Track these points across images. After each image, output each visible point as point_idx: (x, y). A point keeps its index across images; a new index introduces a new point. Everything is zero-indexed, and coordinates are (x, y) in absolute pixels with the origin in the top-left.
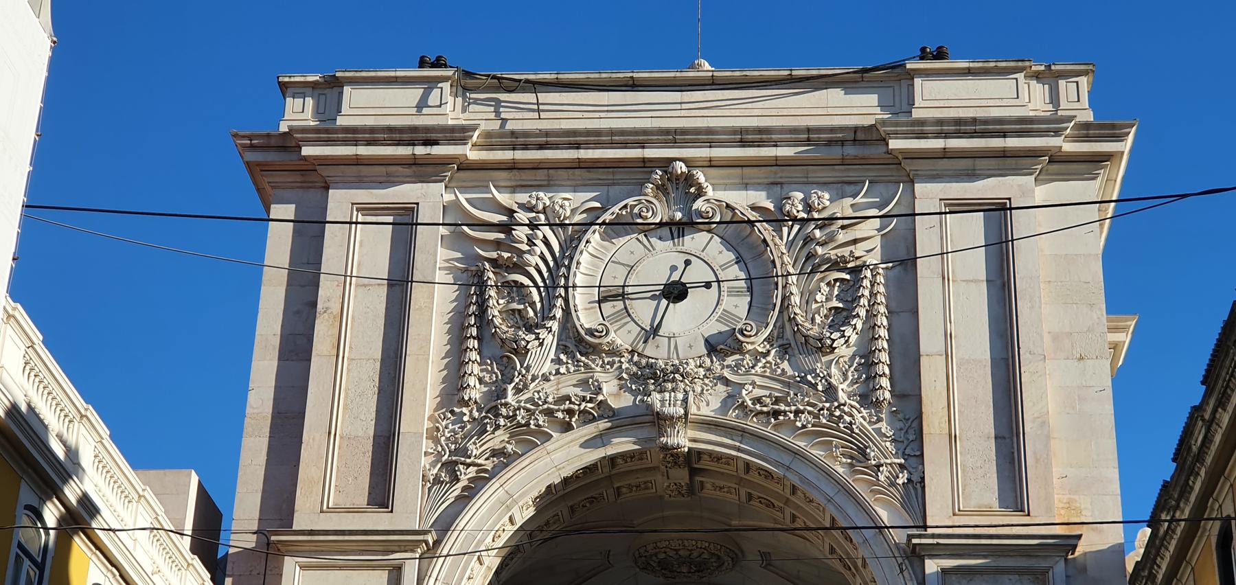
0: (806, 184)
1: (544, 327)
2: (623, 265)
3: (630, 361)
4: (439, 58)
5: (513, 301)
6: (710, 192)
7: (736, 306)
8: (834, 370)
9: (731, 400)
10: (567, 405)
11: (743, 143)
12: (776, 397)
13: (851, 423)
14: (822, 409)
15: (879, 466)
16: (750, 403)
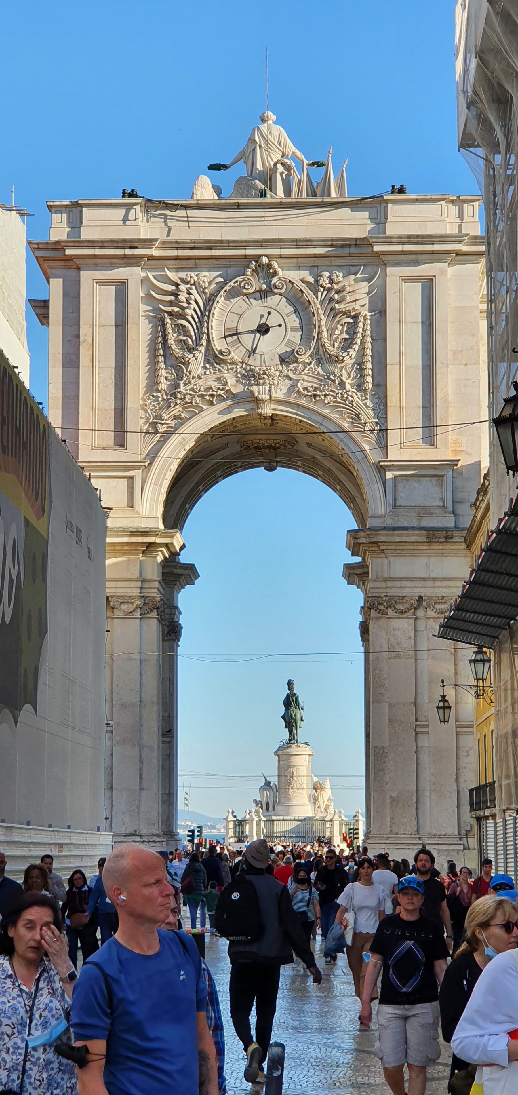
0: (330, 268)
1: (197, 350)
2: (237, 314)
3: (242, 367)
4: (132, 191)
5: (181, 335)
6: (281, 273)
7: (295, 337)
8: (344, 372)
9: (293, 388)
10: (211, 392)
11: (298, 247)
12: (315, 388)
13: (352, 401)
14: (338, 394)
15: (365, 423)
16: (302, 390)
